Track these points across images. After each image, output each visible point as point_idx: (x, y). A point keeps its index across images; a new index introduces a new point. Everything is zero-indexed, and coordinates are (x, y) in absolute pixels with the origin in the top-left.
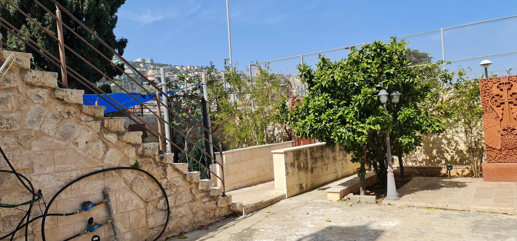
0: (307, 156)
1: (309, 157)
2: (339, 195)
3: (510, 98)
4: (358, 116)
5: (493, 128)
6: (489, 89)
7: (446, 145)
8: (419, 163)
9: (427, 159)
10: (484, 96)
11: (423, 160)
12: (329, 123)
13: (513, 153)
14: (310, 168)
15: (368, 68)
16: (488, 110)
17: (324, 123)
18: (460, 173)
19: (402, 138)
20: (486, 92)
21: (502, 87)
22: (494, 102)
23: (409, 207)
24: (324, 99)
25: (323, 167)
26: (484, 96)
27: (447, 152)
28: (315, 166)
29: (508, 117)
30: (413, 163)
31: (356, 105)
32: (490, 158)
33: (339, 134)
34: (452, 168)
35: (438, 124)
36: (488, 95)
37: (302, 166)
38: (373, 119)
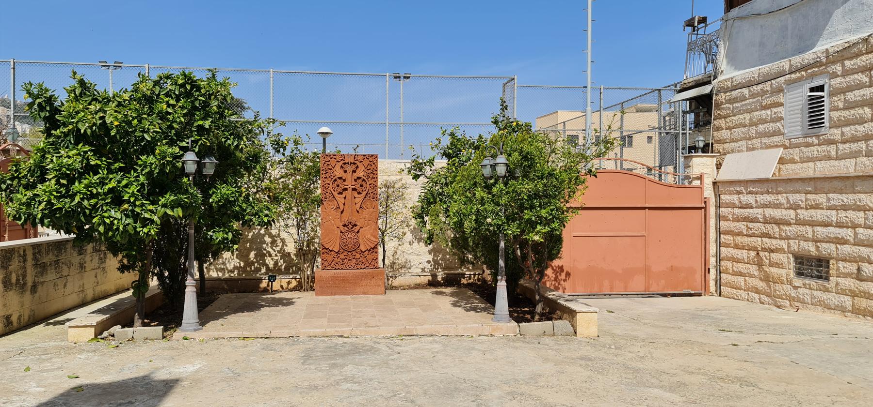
0: (25, 261)
1: (30, 262)
2: (93, 330)
3: (354, 183)
4: (146, 192)
6: (331, 169)
7: (270, 245)
8: (228, 273)
9: (240, 267)
11: (235, 268)
12: (88, 199)
13: (352, 257)
14: (30, 284)
15: (169, 113)
17: (77, 199)
18: (285, 285)
19: (213, 232)
21: (345, 166)
23: (216, 339)
24: (79, 154)
25: (59, 282)
27: (270, 256)
28: (42, 280)
29: (350, 209)
30: (219, 273)
31: (143, 173)
32: (326, 263)
33: (107, 221)
34: (276, 279)
35: (267, 212)
37: (14, 280)
38: (172, 198)
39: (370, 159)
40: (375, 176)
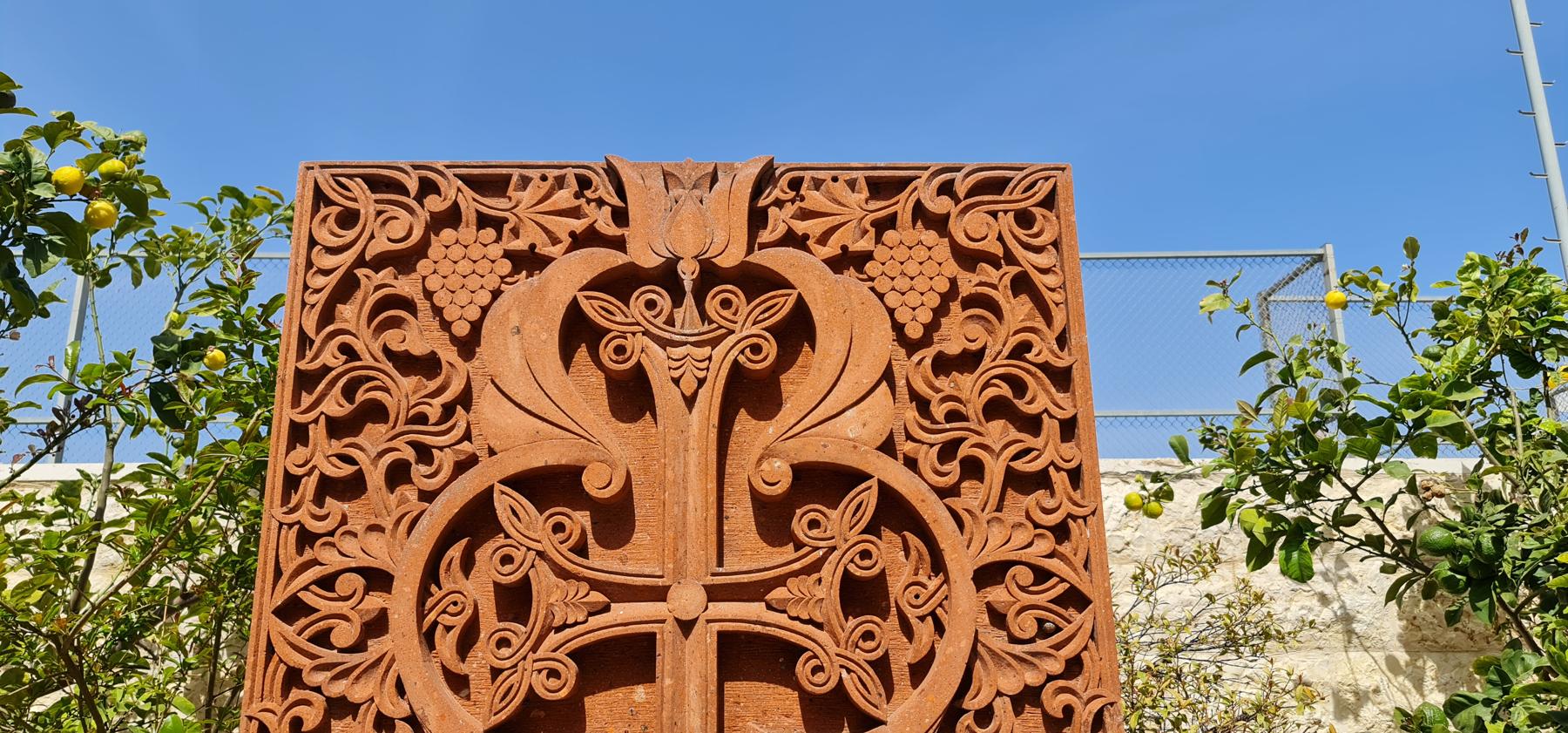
6: (428, 365)
10: (328, 487)
20: (376, 412)
22: (489, 621)
26: (328, 487)
36: (398, 475)
39: (973, 226)
40: (1048, 449)
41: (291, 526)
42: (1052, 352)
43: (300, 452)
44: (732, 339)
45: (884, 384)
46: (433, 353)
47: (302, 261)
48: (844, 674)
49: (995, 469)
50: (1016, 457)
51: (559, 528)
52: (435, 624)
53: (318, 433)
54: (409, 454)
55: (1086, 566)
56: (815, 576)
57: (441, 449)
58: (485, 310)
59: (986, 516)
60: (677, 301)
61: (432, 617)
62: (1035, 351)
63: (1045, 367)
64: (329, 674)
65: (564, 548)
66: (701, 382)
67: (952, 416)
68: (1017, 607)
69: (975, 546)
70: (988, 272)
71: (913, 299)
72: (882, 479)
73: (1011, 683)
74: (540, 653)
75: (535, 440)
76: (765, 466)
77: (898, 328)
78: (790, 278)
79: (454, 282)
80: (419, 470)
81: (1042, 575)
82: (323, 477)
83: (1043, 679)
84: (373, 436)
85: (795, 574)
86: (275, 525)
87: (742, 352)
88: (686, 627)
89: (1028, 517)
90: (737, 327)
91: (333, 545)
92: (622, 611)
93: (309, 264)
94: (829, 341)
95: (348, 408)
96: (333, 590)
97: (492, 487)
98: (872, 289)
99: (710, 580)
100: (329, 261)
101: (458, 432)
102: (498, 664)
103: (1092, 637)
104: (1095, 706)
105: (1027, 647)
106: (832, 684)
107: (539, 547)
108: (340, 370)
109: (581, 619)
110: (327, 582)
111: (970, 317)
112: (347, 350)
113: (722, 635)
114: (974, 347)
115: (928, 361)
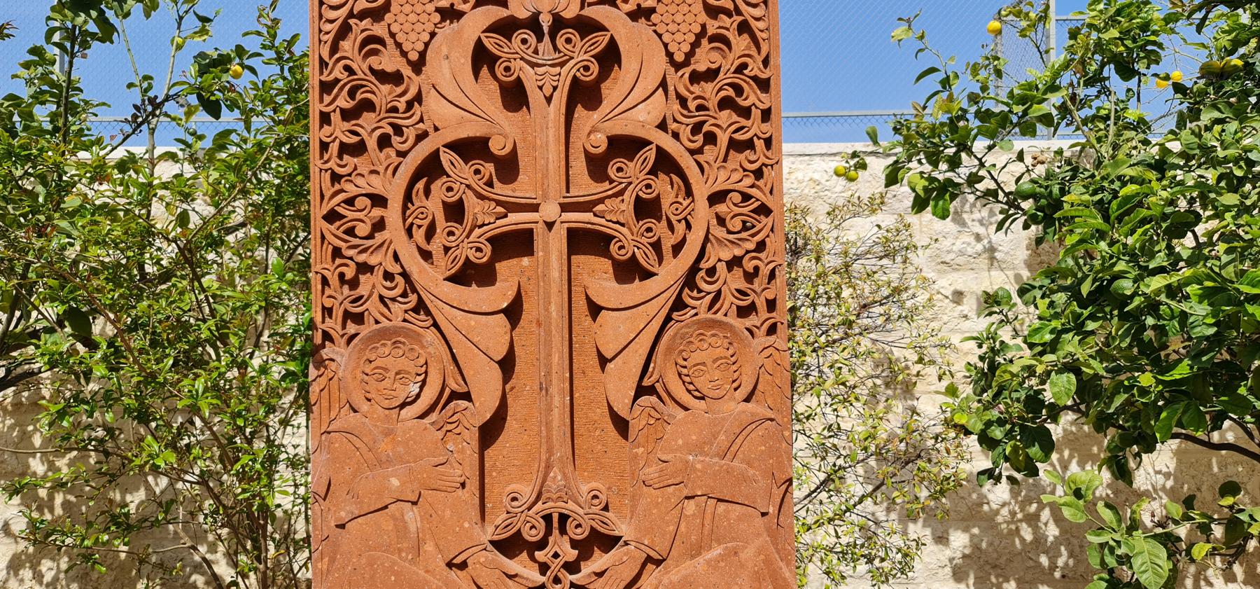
3: (585, 187)
5: (401, 527)
6: (395, 78)
10: (344, 149)
16: (373, 306)
20: (368, 106)
21: (512, 50)
22: (441, 223)
26: (344, 149)
29: (559, 400)
36: (384, 142)
40: (755, 127)
41: (326, 171)
42: (760, 69)
43: (327, 129)
44: (572, 63)
45: (661, 89)
46: (398, 71)
47: (316, 14)
48: (636, 249)
49: (723, 139)
50: (736, 131)
51: (477, 172)
52: (412, 224)
53: (336, 117)
54: (389, 130)
55: (771, 192)
56: (620, 198)
57: (407, 127)
58: (427, 45)
59: (717, 165)
60: (540, 39)
61: (410, 220)
62: (749, 68)
63: (755, 79)
64: (357, 251)
65: (481, 183)
66: (555, 88)
67: (700, 108)
68: (732, 214)
69: (710, 181)
70: (724, 20)
71: (679, 37)
72: (661, 145)
73: (727, 255)
74: (471, 239)
75: (461, 122)
76: (592, 137)
77: (670, 55)
78: (606, 24)
79: (407, 27)
80: (396, 140)
81: (746, 197)
82: (342, 144)
83: (744, 252)
84: (368, 119)
85: (609, 197)
86: (317, 170)
87: (578, 70)
88: (550, 225)
89: (741, 166)
90: (575, 55)
91: (351, 181)
92: (513, 217)
93: (321, 16)
94: (629, 64)
95: (352, 103)
96: (354, 206)
97: (438, 149)
98: (655, 31)
99: (562, 200)
100: (332, 14)
101: (416, 118)
102: (448, 244)
103: (772, 230)
104: (771, 266)
105: (736, 236)
106: (629, 255)
107: (467, 182)
108: (346, 81)
109: (492, 221)
110: (350, 202)
111: (713, 48)
112: (348, 69)
113: (570, 230)
114: (714, 66)
115: (687, 75)
